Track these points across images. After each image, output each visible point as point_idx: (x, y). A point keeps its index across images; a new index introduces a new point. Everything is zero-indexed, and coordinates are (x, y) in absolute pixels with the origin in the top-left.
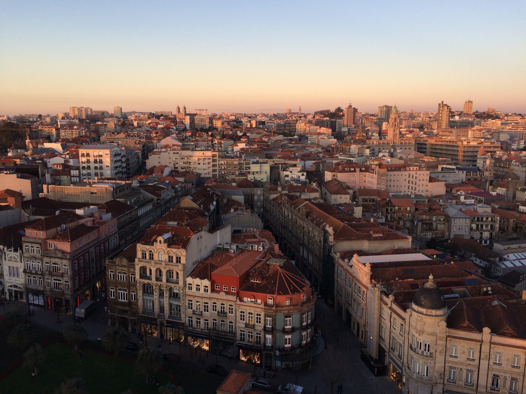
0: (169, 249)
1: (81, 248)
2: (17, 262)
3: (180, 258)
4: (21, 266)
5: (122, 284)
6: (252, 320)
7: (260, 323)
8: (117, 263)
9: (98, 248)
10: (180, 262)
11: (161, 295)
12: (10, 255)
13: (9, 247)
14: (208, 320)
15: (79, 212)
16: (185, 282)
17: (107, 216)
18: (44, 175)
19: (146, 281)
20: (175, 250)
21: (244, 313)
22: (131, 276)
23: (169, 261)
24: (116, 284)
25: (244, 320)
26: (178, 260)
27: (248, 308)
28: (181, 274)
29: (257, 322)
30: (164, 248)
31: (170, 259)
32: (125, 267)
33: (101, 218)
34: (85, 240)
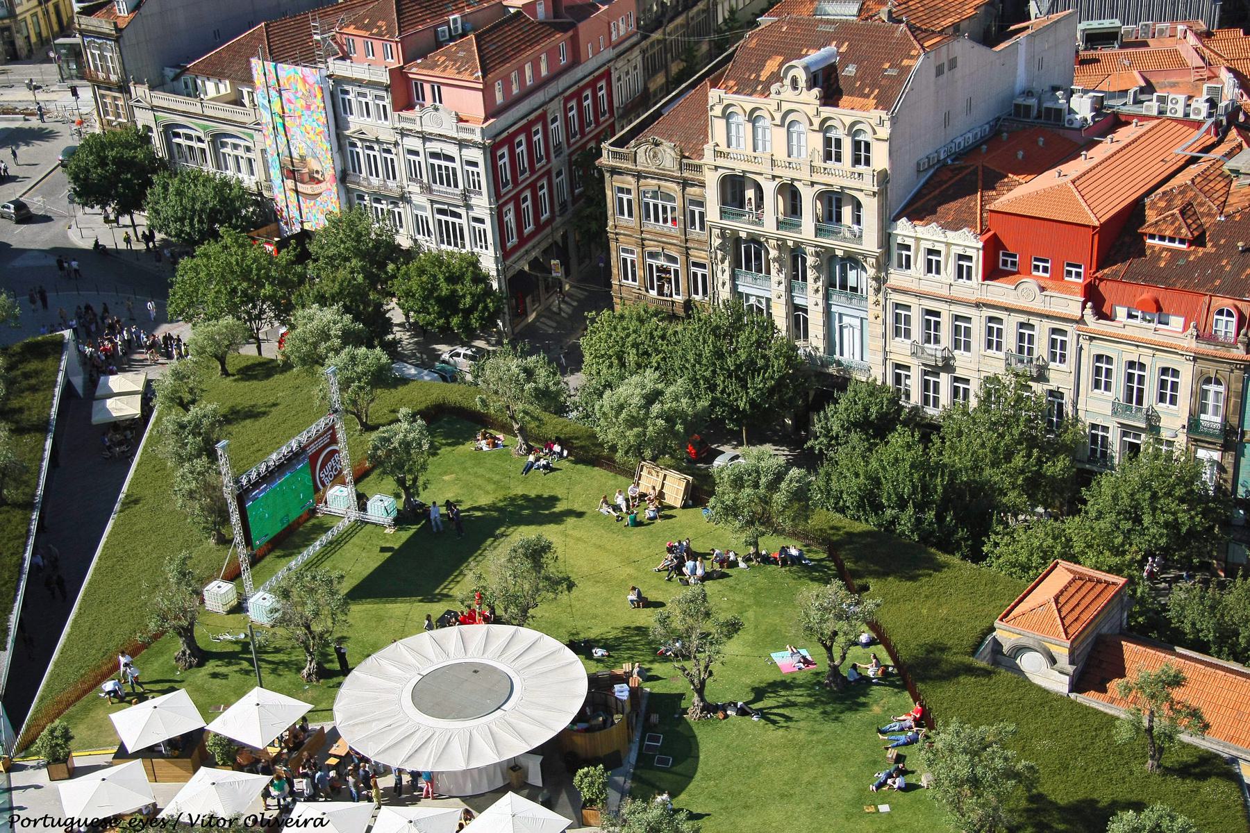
0: (827, 111)
6: (1140, 391)
7: (1173, 401)
9: (574, 103)
10: (867, 163)
14: (967, 381)
16: (886, 239)
23: (828, 157)
28: (871, 207)
29: (1162, 398)
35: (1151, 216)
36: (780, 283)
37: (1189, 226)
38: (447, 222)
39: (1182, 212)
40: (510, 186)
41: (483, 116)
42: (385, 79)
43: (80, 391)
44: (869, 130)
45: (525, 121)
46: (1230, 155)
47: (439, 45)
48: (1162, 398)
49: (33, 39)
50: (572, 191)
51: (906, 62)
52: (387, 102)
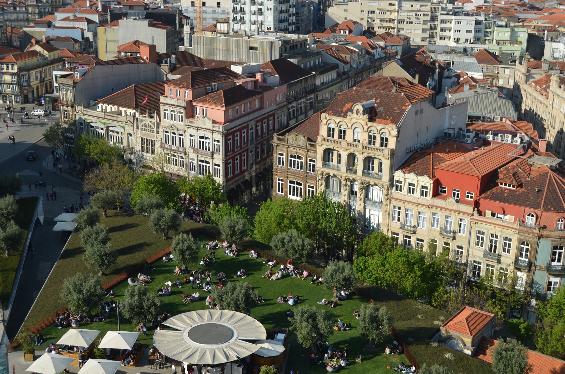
0: (370, 124)
2: (153, 132)
6: (495, 247)
7: (509, 252)
8: (290, 141)
9: (259, 124)
10: (386, 146)
12: (144, 122)
13: (143, 112)
14: (422, 241)
15: (237, 69)
16: (392, 178)
18: (182, 26)
20: (379, 127)
21: (483, 233)
26: (384, 142)
27: (492, 227)
28: (386, 164)
29: (504, 250)
30: (363, 122)
31: (371, 140)
32: (299, 147)
34: (243, 107)
35: (501, 176)
36: (345, 195)
37: (516, 181)
38: (203, 166)
39: (514, 175)
40: (232, 152)
41: (223, 121)
42: (184, 104)
43: (42, 223)
44: (388, 133)
45: (240, 127)
46: (530, 157)
47: (207, 94)
48: (504, 250)
49: (35, 95)
50: (256, 159)
51: (403, 108)
52: (184, 115)
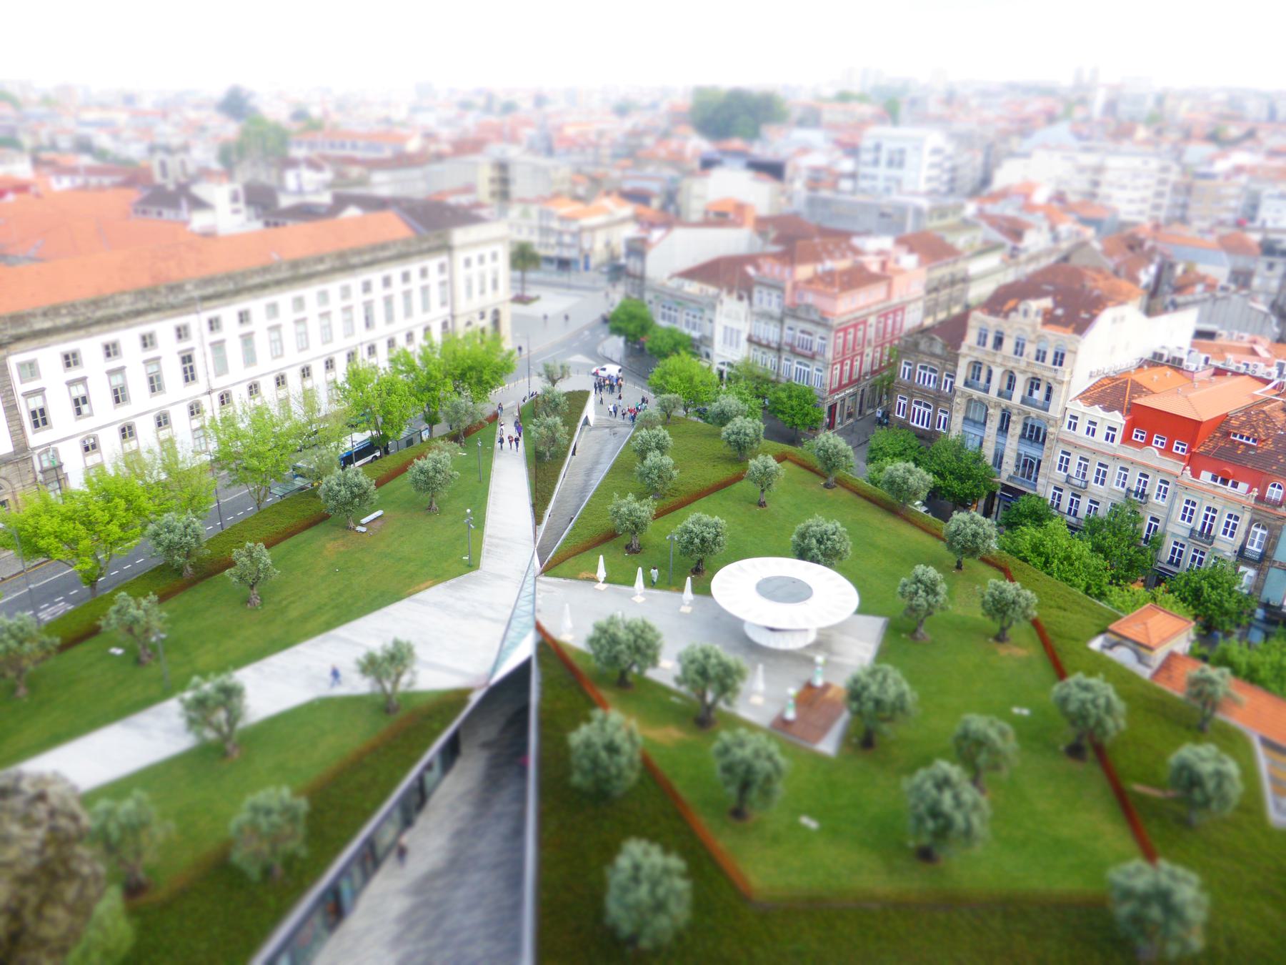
1: (852, 312)
3: (1063, 355)
4: (745, 328)
5: (924, 392)
6: (1211, 526)
7: (1232, 535)
11: (1004, 428)
13: (730, 292)
17: (909, 261)
18: (792, 181)
19: (976, 394)
22: (945, 378)
24: (910, 390)
25: (1190, 520)
32: (933, 355)
33: (897, 261)
